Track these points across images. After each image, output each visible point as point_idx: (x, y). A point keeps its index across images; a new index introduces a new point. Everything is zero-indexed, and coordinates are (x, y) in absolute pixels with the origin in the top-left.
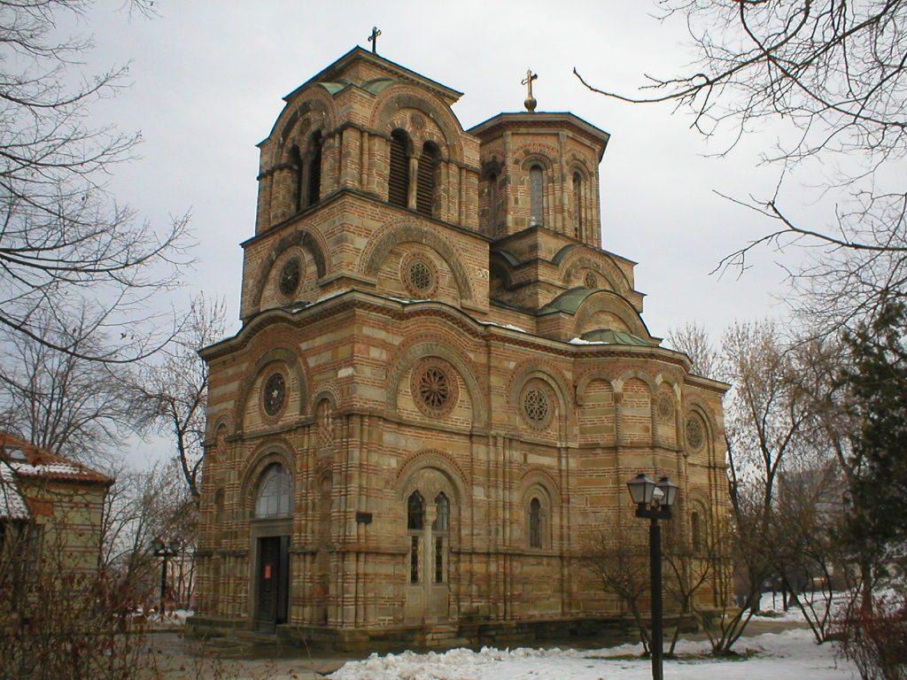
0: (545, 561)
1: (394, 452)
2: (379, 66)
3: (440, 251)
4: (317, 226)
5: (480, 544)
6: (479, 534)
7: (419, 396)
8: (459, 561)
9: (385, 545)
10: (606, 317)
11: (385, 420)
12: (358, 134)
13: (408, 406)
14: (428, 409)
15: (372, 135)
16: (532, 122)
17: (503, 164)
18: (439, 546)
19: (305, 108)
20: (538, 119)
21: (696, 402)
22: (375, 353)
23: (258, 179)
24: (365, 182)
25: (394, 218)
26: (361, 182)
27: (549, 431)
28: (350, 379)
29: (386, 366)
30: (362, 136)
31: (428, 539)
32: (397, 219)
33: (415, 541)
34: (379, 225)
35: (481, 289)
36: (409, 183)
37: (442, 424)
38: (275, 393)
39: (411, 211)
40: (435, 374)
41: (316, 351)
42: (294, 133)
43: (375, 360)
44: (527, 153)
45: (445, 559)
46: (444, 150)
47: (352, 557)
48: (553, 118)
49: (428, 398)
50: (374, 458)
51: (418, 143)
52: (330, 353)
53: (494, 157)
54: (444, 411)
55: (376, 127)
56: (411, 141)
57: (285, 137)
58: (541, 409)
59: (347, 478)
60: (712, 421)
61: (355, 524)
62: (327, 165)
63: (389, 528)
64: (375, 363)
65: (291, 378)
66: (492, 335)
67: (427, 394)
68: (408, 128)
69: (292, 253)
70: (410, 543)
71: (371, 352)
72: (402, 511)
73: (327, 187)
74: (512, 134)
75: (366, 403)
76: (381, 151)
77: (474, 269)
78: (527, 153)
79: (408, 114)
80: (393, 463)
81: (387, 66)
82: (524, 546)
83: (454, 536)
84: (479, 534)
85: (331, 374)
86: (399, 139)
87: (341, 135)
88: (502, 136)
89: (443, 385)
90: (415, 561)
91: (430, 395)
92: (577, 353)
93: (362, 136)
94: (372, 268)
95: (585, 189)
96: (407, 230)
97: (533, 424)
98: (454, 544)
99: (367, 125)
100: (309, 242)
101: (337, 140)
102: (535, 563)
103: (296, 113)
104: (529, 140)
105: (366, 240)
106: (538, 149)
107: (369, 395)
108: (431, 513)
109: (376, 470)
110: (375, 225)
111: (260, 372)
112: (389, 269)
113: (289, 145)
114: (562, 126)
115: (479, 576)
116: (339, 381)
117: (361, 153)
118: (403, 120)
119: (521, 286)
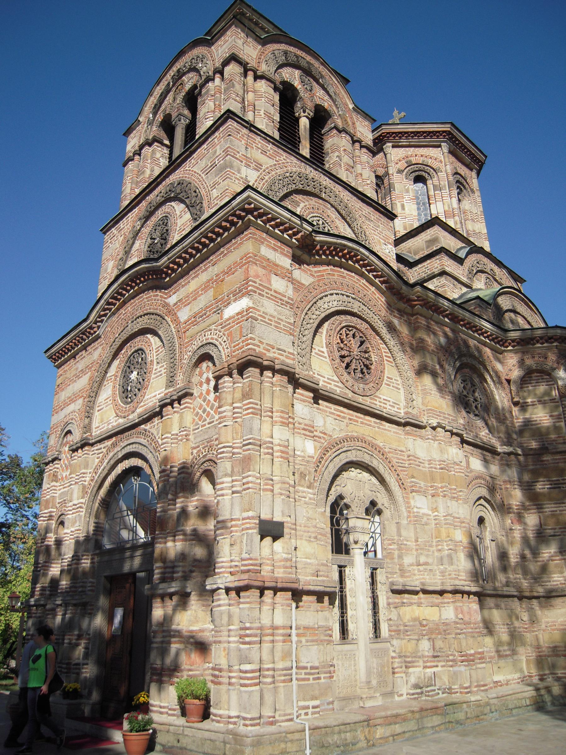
1: (309, 431)
3: (343, 212)
6: (426, 564)
7: (338, 360)
32: (290, 164)
37: (366, 402)
43: (279, 294)
44: (410, 164)
45: (382, 601)
52: (211, 292)
55: (263, 68)
67: (347, 360)
68: (297, 84)
70: (336, 576)
71: (272, 282)
75: (268, 351)
77: (380, 241)
86: (287, 96)
89: (366, 352)
90: (343, 607)
103: (169, 84)
111: (115, 356)
116: (225, 325)
118: (293, 76)
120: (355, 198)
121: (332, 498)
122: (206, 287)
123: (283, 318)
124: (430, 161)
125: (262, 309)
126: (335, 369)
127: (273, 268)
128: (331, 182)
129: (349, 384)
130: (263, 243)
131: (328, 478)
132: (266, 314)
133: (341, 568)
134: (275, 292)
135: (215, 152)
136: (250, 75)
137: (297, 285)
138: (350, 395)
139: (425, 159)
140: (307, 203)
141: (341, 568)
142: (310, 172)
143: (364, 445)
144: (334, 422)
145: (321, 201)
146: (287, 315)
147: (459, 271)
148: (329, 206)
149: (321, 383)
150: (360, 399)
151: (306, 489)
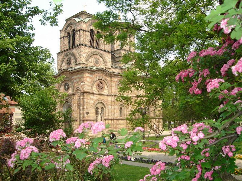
0: (123, 120)
1: (92, 99)
3: (101, 56)
4: (75, 51)
5: (110, 118)
8: (106, 121)
9: (92, 118)
13: (95, 90)
14: (99, 90)
18: (102, 118)
19: (71, 24)
22: (89, 80)
23: (60, 38)
24: (85, 42)
26: (84, 42)
28: (84, 85)
29: (90, 82)
30: (84, 31)
31: (99, 116)
32: (92, 50)
34: (88, 51)
38: (67, 87)
41: (76, 79)
42: (69, 29)
50: (89, 101)
51: (95, 32)
55: (87, 30)
57: (66, 30)
59: (84, 105)
61: (85, 114)
62: (76, 38)
63: (92, 115)
64: (89, 82)
65: (70, 84)
66: (112, 74)
69: (69, 57)
70: (96, 117)
72: (94, 111)
73: (77, 43)
76: (88, 34)
80: (92, 102)
82: (119, 118)
83: (105, 116)
85: (79, 84)
87: (79, 31)
93: (84, 31)
94: (87, 61)
96: (94, 52)
98: (105, 118)
100: (73, 55)
101: (79, 32)
103: (68, 24)
105: (85, 55)
107: (87, 88)
108: (100, 111)
109: (89, 104)
110: (87, 51)
113: (67, 32)
119: (118, 61)
121: (96, 107)
122: (78, 78)
127: (88, 77)
131: (95, 105)
133: (97, 117)
135: (79, 51)
136: (85, 31)
138: (99, 93)
141: (97, 117)
142: (95, 50)
146: (90, 84)
150: (100, 93)
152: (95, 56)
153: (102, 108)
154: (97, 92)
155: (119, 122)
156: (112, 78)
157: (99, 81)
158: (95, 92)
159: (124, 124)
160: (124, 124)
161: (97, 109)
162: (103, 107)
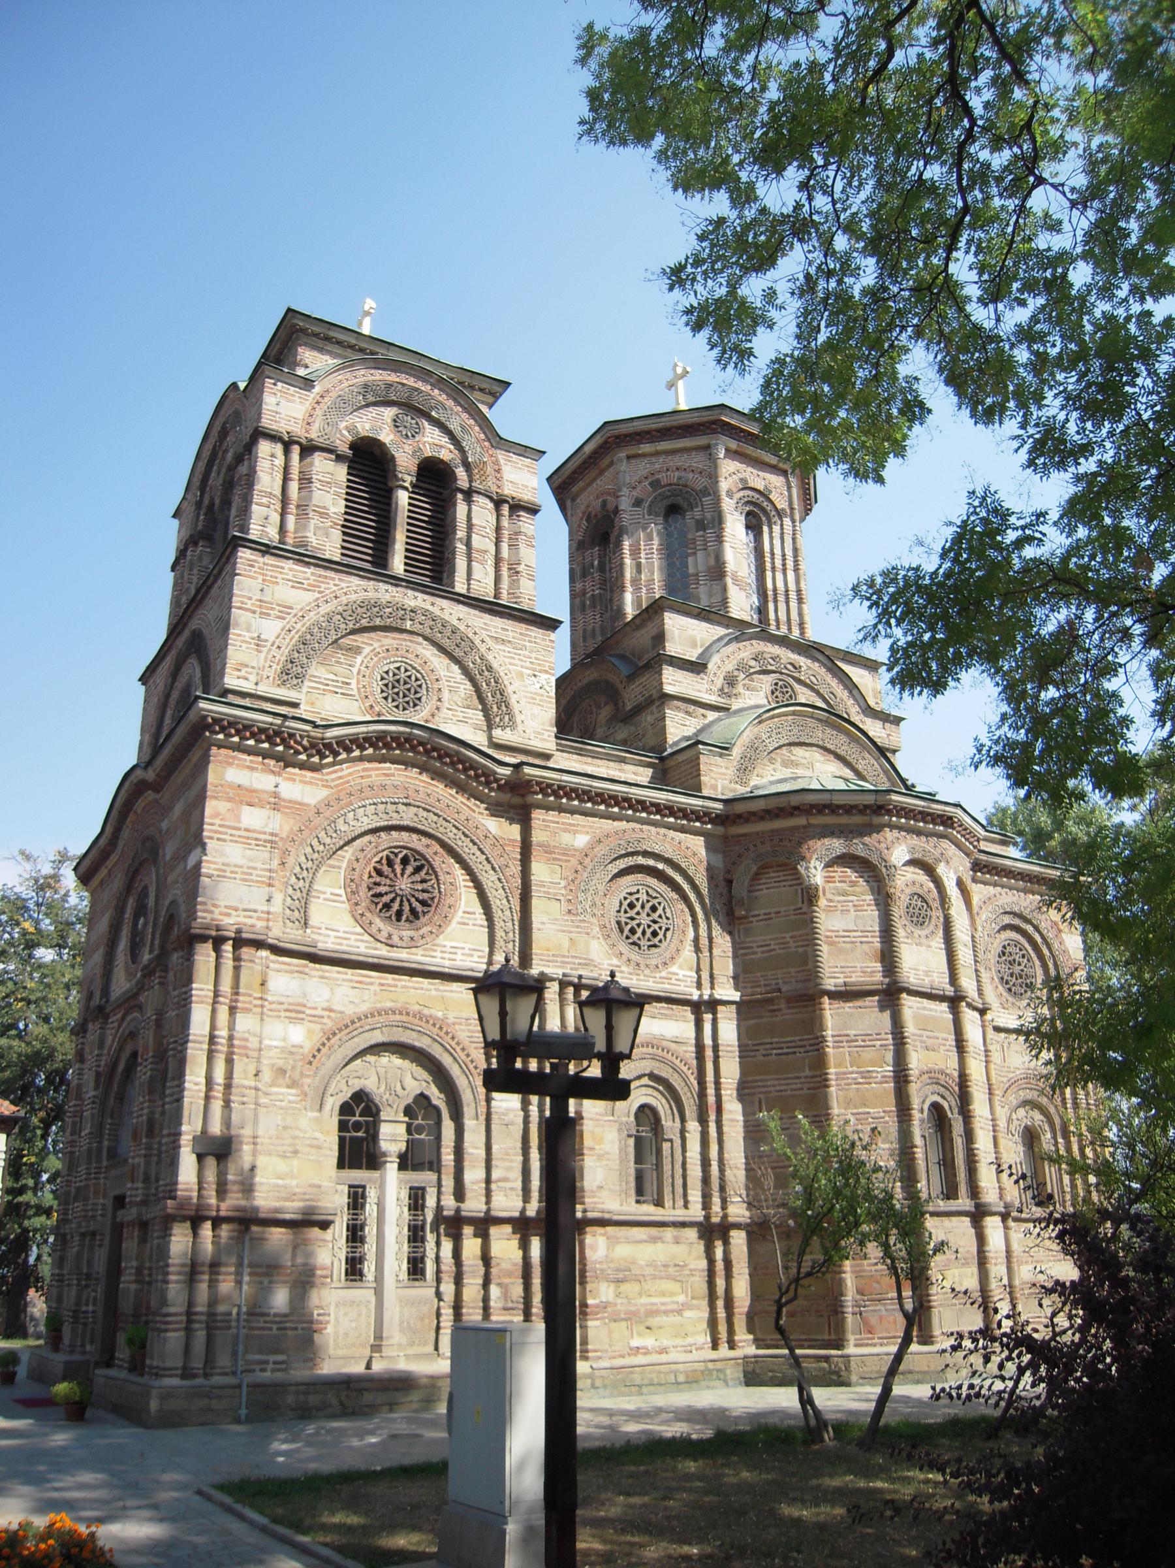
0: (669, 1233)
1: (296, 1012)
2: (339, 343)
3: (446, 643)
6: (505, 1180)
10: (807, 754)
11: (276, 950)
12: (279, 449)
13: (335, 923)
15: (308, 449)
16: (658, 431)
17: (616, 511)
20: (668, 424)
21: (1016, 909)
25: (343, 585)
27: (674, 969)
30: (287, 452)
32: (356, 589)
33: (357, 1198)
34: (310, 597)
35: (536, 710)
36: (388, 531)
39: (395, 580)
40: (405, 861)
44: (655, 484)
46: (461, 472)
47: (208, 1225)
48: (695, 418)
49: (387, 906)
51: (406, 462)
53: (604, 503)
54: (425, 930)
56: (393, 457)
58: (656, 927)
60: (1056, 946)
68: (387, 436)
74: (628, 457)
75: (228, 915)
76: (331, 484)
77: (521, 675)
78: (655, 484)
79: (389, 413)
81: (353, 341)
84: (505, 1180)
86: (368, 462)
88: (612, 463)
89: (423, 881)
91: (393, 900)
92: (727, 817)
94: (292, 672)
95: (771, 538)
97: (635, 957)
99: (298, 430)
102: (644, 1237)
104: (659, 463)
105: (279, 624)
106: (675, 476)
108: (392, 1136)
110: (300, 598)
112: (332, 677)
114: (714, 432)
115: (504, 1265)
117: (286, 479)
118: (379, 424)
119: (639, 709)
120: (477, 612)
123: (259, 865)
124: (691, 475)
125: (220, 860)
126: (359, 919)
127: (247, 797)
128: (426, 597)
129: (383, 936)
130: (231, 764)
132: (228, 865)
134: (247, 830)
137: (296, 808)
139: (683, 474)
140: (376, 645)
143: (404, 1018)
144: (351, 992)
145: (404, 636)
146: (261, 859)
147: (698, 687)
148: (420, 639)
149: (320, 945)
150: (403, 955)
151: (284, 1090)
152: (389, 640)
153: (419, 1108)
154: (361, 946)
155: (623, 1251)
156: (538, 816)
157: (386, 840)
158: (327, 943)
159: (674, 1271)
160: (674, 1271)
161: (359, 1113)
162: (437, 1097)
